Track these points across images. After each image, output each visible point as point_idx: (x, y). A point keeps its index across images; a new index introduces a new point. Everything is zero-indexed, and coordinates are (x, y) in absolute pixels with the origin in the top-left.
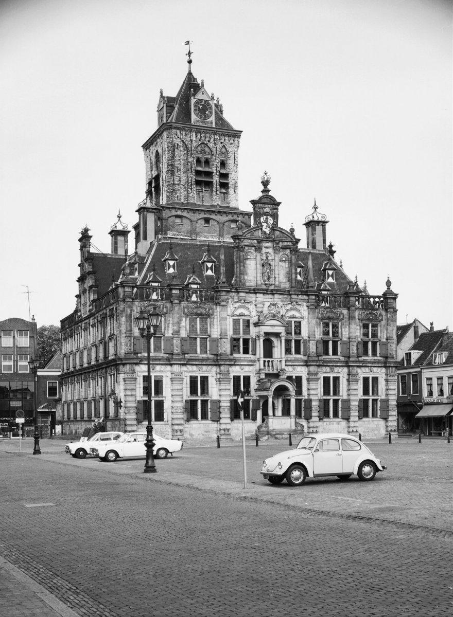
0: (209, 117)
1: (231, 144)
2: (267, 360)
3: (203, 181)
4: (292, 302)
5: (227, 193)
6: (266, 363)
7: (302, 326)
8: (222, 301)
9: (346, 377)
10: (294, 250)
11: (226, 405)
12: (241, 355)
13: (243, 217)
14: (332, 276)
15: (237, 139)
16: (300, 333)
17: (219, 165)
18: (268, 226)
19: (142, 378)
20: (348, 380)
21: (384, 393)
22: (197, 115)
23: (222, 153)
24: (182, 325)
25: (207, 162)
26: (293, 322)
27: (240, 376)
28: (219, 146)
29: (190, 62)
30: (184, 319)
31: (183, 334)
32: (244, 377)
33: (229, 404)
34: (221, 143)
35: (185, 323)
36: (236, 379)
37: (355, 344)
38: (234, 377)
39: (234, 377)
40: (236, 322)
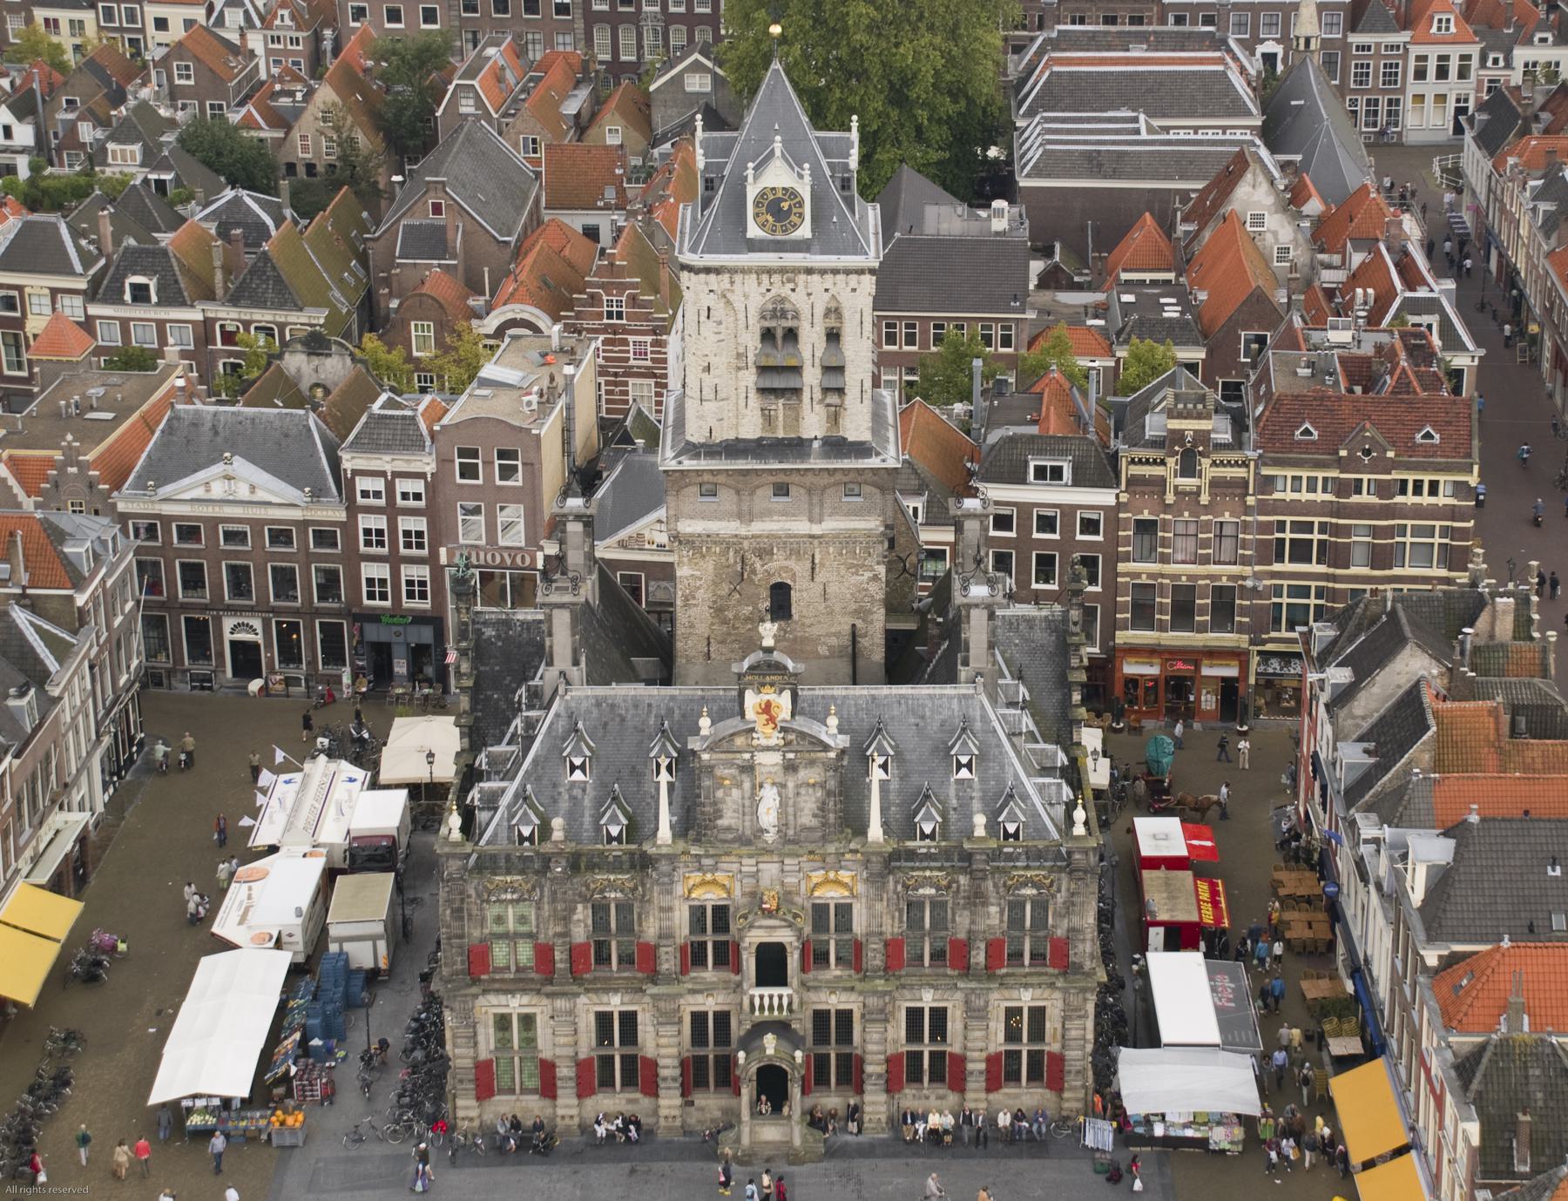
0: (795, 226)
1: (854, 290)
2: (757, 992)
3: (777, 381)
6: (757, 1002)
11: (669, 1069)
16: (850, 930)
17: (821, 344)
22: (763, 226)
23: (828, 312)
24: (575, 917)
25: (791, 335)
27: (706, 1014)
30: (580, 907)
33: (677, 1072)
35: (582, 913)
36: (699, 1019)
37: (983, 946)
38: (693, 1014)
39: (693, 1014)
40: (698, 913)
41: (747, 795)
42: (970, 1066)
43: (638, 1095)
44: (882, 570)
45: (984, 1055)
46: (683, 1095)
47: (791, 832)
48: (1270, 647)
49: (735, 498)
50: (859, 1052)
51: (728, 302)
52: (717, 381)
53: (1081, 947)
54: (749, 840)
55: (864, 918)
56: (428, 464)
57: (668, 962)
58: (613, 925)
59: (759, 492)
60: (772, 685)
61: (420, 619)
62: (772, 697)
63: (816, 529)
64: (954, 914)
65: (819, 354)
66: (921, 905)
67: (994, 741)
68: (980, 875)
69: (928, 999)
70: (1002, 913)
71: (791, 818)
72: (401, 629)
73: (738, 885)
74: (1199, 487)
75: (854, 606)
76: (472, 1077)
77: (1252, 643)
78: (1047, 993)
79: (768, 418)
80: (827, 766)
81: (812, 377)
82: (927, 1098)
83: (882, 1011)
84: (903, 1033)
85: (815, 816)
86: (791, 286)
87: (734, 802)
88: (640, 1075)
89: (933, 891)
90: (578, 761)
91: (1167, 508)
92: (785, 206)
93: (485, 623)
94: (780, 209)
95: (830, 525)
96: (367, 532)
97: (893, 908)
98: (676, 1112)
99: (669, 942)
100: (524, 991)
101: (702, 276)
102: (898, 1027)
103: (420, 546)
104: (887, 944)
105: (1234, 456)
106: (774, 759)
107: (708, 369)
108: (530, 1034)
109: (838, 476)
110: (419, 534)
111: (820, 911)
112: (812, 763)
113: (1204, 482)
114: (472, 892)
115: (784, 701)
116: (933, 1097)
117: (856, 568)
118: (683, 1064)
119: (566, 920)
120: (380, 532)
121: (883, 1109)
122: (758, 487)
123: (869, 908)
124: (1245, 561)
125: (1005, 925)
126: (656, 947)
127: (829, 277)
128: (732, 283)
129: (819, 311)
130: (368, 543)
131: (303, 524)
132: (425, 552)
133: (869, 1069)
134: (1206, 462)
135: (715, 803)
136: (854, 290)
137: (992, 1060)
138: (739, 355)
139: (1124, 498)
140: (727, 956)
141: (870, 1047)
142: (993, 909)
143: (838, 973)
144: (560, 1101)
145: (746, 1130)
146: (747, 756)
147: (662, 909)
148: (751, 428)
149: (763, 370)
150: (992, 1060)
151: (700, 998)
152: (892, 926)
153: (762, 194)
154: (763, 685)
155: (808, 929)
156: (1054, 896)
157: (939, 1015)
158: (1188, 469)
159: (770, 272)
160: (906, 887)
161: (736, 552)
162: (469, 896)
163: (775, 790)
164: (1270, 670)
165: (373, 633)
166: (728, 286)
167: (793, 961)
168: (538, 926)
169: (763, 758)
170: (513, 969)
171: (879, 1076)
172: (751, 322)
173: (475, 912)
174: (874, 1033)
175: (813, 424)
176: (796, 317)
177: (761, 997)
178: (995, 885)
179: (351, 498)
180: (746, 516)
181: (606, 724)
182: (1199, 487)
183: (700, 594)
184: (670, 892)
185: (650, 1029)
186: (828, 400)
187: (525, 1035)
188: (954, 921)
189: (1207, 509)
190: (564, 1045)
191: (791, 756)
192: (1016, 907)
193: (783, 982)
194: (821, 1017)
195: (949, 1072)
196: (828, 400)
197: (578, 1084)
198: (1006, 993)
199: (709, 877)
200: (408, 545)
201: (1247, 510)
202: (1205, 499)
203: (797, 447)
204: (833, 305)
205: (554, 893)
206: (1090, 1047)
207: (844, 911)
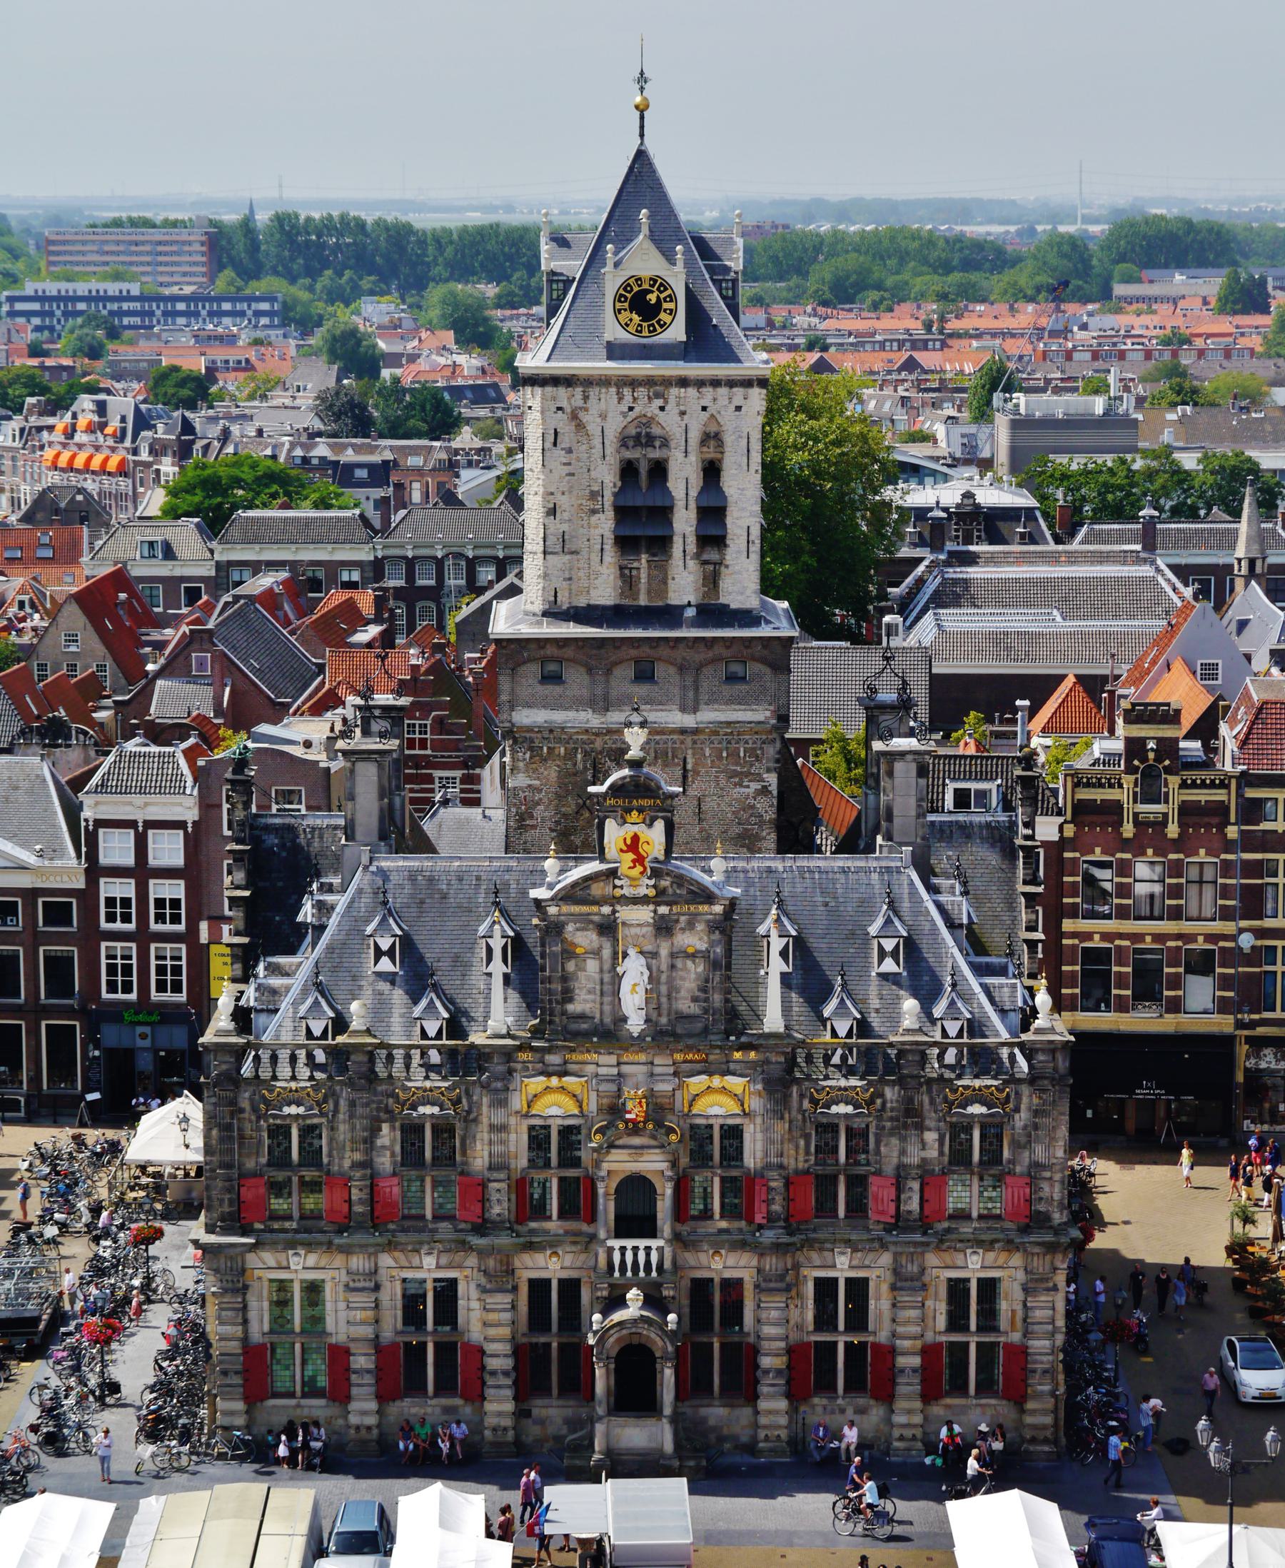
1: (738, 408)
2: (616, 1244)
5: (720, 563)
7: (747, 1137)
9: (889, 1277)
11: (499, 1359)
12: (554, 1225)
13: (765, 647)
14: (895, 954)
18: (640, 860)
19: (266, 1284)
20: (893, 1288)
21: (1019, 1323)
24: (379, 1142)
25: (659, 470)
27: (548, 1281)
28: (696, 425)
29: (642, 110)
30: (385, 1128)
31: (385, 1162)
32: (560, 1281)
34: (704, 409)
35: (387, 1136)
37: (916, 1185)
41: (607, 966)
42: (902, 1361)
43: (458, 1401)
44: (772, 779)
45: (919, 1343)
46: (516, 1398)
47: (664, 1020)
48: (1261, 1031)
49: (586, 679)
50: (751, 1339)
51: (580, 426)
52: (565, 527)
53: (1045, 1186)
54: (609, 1034)
55: (759, 1146)
56: (187, 809)
57: (499, 1207)
58: (428, 1154)
59: (618, 672)
60: (640, 810)
61: (169, 1014)
62: (641, 829)
63: (689, 721)
64: (878, 1143)
65: (693, 493)
66: (834, 1128)
67: (927, 927)
68: (913, 1083)
69: (843, 1266)
70: (941, 1141)
71: (664, 1000)
72: (147, 1030)
73: (593, 1095)
74: (1165, 815)
75: (737, 830)
76: (239, 1367)
77: (1240, 1025)
78: (1003, 1257)
79: (628, 580)
80: (714, 926)
81: (684, 522)
82: (843, 1411)
83: (781, 1278)
84: (810, 1316)
86: (660, 402)
87: (588, 978)
88: (460, 1370)
90: (385, 944)
91: (1125, 845)
92: (652, 298)
93: (268, 828)
94: (648, 302)
95: (709, 715)
96: (110, 902)
97: (796, 1133)
98: (508, 1422)
99: (502, 1176)
100: (310, 1246)
101: (549, 389)
103: (176, 919)
104: (788, 1183)
105: (1206, 775)
106: (643, 914)
107: (552, 512)
108: (316, 1312)
109: (719, 650)
110: (175, 903)
111: (699, 1137)
113: (1170, 808)
114: (245, 1104)
115: (654, 838)
116: (850, 1411)
117: (739, 778)
118: (518, 1352)
119: (369, 1142)
120: (126, 902)
121: (783, 1421)
122: (616, 664)
123: (766, 1130)
124: (1226, 914)
125: (946, 1159)
126: (483, 1184)
127: (708, 391)
128: (586, 398)
129: (695, 436)
130: (111, 918)
131: (31, 894)
132: (181, 927)
133: (766, 1362)
134: (1174, 781)
135: (565, 979)
136: (738, 408)
137: (930, 1352)
138: (593, 495)
139: (1070, 831)
140: (578, 1201)
141: (768, 1330)
142: (931, 1136)
143: (724, 1224)
144: (354, 1406)
145: (600, 1428)
146: (606, 910)
147: (492, 1128)
148: (605, 592)
149: (623, 513)
150: (930, 1352)
151: (540, 1259)
152: (798, 1158)
153: (626, 286)
154: (629, 811)
155: (684, 1161)
156: (1009, 1116)
157: (858, 1289)
158: (1150, 793)
159: (633, 383)
160: (815, 1102)
161: (586, 754)
162: (242, 1111)
163: (642, 960)
164: (1263, 1065)
165: (111, 1035)
166: (580, 403)
167: (664, 1206)
168: (330, 1155)
169: (627, 914)
170: (296, 1214)
171: (779, 1372)
172: (608, 452)
173: (248, 1132)
174: (773, 1308)
175: (684, 586)
176: (665, 443)
177: (623, 1249)
178: (932, 1102)
179: (92, 856)
180: (603, 704)
181: (422, 902)
182: (1165, 815)
183: (539, 811)
184: (502, 1103)
185: (475, 1305)
186: (705, 557)
187: (310, 1312)
188: (878, 1152)
189: (1178, 845)
190: (363, 1323)
191: (663, 910)
192: (959, 1130)
193: (653, 1234)
194: (701, 1288)
195: (872, 1373)
196: (705, 557)
197: (379, 1380)
198: (947, 1257)
199: (554, 1081)
200: (160, 918)
201: (1229, 846)
202: (1173, 830)
203: (670, 615)
204: (713, 429)
205: (352, 1104)
206: (1060, 1339)
207: (733, 1134)
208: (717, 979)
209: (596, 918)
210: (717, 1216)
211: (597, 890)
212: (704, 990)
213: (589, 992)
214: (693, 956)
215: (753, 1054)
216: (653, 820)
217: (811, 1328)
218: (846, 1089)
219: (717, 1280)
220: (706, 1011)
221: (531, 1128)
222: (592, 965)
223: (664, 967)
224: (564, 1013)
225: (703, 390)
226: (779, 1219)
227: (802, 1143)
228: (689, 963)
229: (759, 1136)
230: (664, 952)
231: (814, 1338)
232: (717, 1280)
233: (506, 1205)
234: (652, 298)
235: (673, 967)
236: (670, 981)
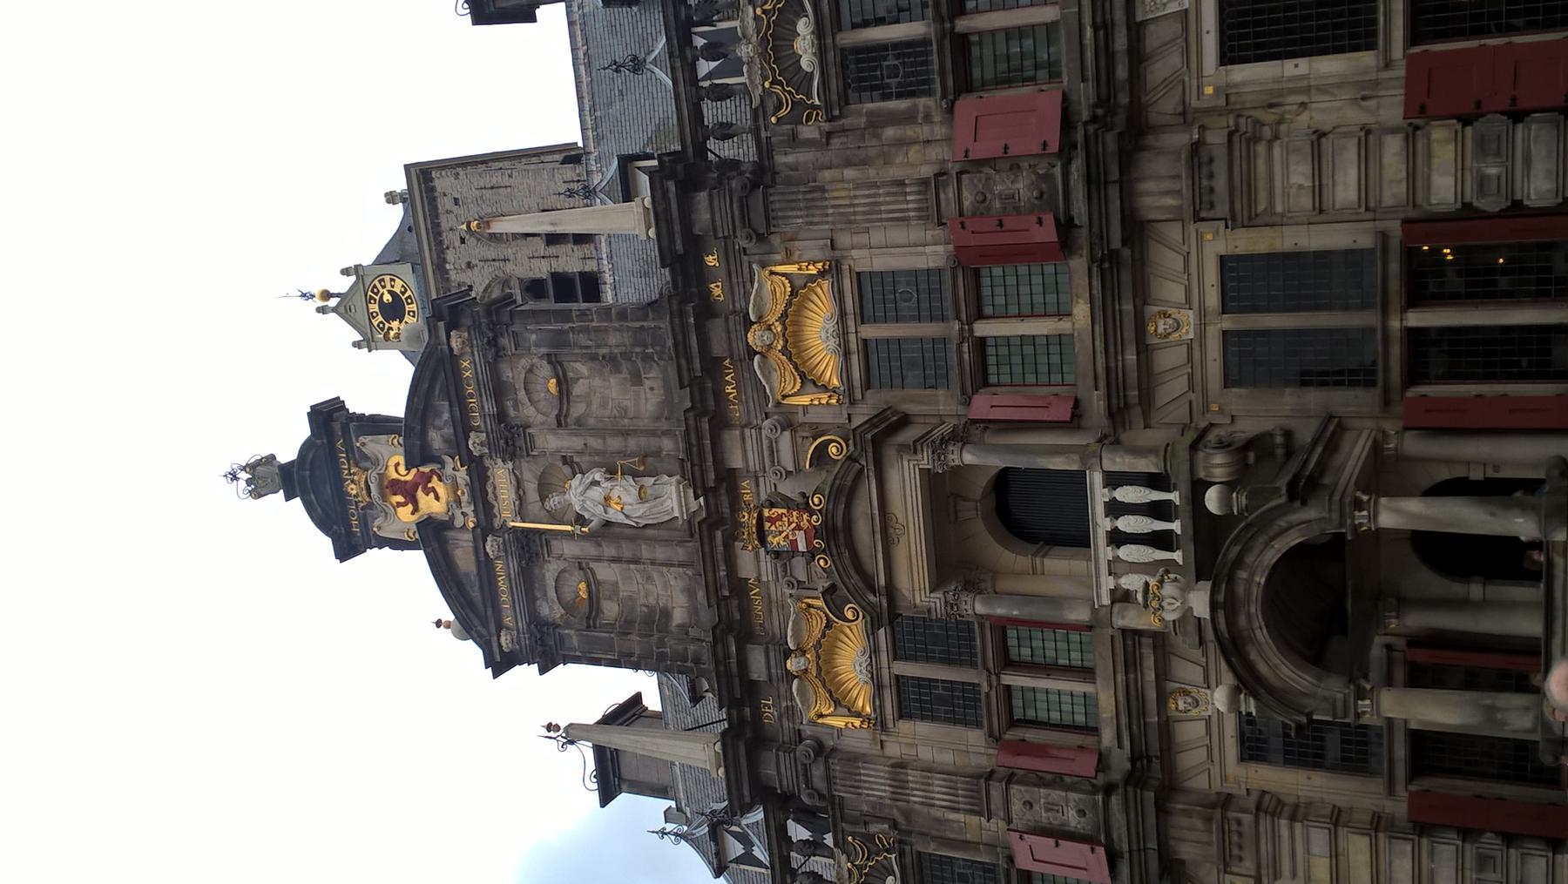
1: (456, 200)
4: (752, 353)
7: (881, 263)
8: (808, 782)
10: (493, 343)
15: (442, 183)
26: (870, 331)
28: (476, 251)
34: (463, 241)
47: (667, 444)
50: (1394, 227)
55: (898, 235)
84: (1329, 66)
85: (637, 379)
89: (804, 27)
102: (1306, 88)
112: (499, 391)
127: (450, 238)
133: (1443, 190)
135: (625, 626)
136: (456, 200)
141: (1345, 190)
143: (1081, 311)
151: (1190, 732)
160: (800, 112)
176: (506, 283)
208: (582, 339)
209: (514, 565)
210: (1064, 326)
211: (464, 559)
212: (612, 362)
213: (649, 578)
214: (564, 384)
215: (711, 261)
216: (366, 457)
217: (1367, 58)
218: (764, 40)
219: (1228, 322)
220: (647, 358)
221: (903, 713)
222: (605, 572)
223: (577, 443)
224: (684, 628)
225: (446, 243)
226: (1048, 177)
227: (890, 132)
228: (578, 389)
229: (877, 237)
230: (551, 442)
231: (1398, 50)
232: (1228, 322)
233: (1056, 795)
234: (387, 298)
235: (579, 422)
236: (601, 432)
